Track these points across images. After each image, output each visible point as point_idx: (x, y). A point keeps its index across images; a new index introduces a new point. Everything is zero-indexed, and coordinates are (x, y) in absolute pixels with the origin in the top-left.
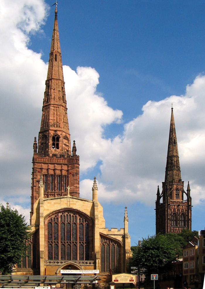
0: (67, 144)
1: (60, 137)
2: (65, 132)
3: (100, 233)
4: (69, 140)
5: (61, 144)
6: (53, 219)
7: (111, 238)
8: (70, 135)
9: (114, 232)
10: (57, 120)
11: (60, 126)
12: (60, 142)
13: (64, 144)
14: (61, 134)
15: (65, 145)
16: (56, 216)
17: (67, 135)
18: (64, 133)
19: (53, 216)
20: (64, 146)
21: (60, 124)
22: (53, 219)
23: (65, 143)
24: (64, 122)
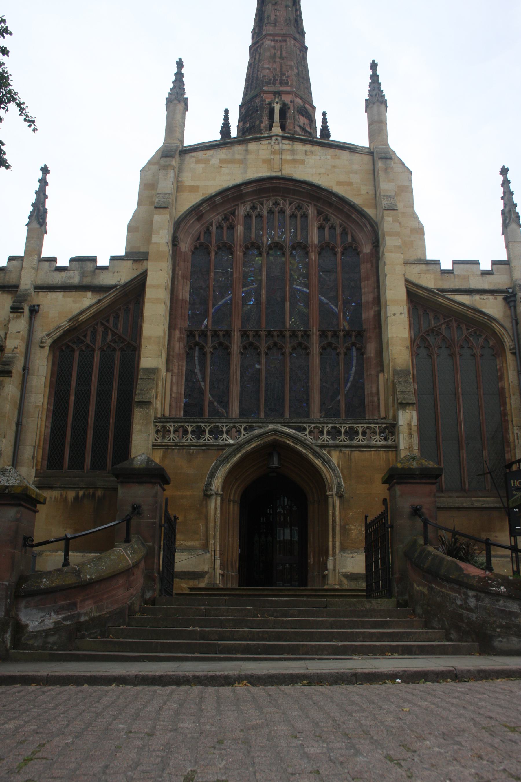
0: (308, 129)
1: (289, 108)
2: (301, 98)
3: (411, 287)
4: (313, 119)
5: (292, 125)
6: (214, 229)
7: (455, 306)
8: (314, 108)
9: (466, 278)
10: (281, 69)
11: (287, 83)
12: (288, 121)
13: (300, 127)
14: (291, 102)
15: (303, 129)
16: (226, 219)
17: (307, 106)
18: (298, 101)
19: (215, 218)
20: (298, 129)
21: (288, 77)
22: (214, 229)
23: (301, 124)
24: (298, 74)
